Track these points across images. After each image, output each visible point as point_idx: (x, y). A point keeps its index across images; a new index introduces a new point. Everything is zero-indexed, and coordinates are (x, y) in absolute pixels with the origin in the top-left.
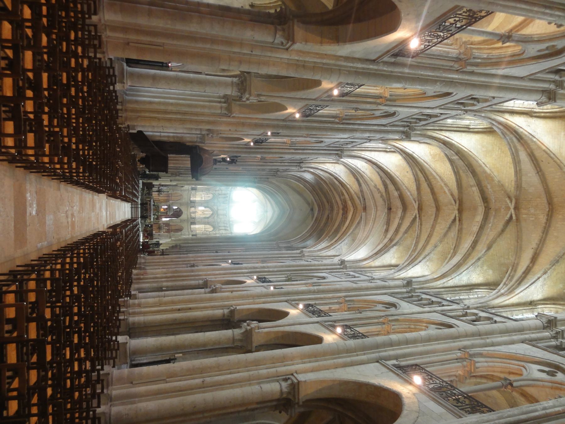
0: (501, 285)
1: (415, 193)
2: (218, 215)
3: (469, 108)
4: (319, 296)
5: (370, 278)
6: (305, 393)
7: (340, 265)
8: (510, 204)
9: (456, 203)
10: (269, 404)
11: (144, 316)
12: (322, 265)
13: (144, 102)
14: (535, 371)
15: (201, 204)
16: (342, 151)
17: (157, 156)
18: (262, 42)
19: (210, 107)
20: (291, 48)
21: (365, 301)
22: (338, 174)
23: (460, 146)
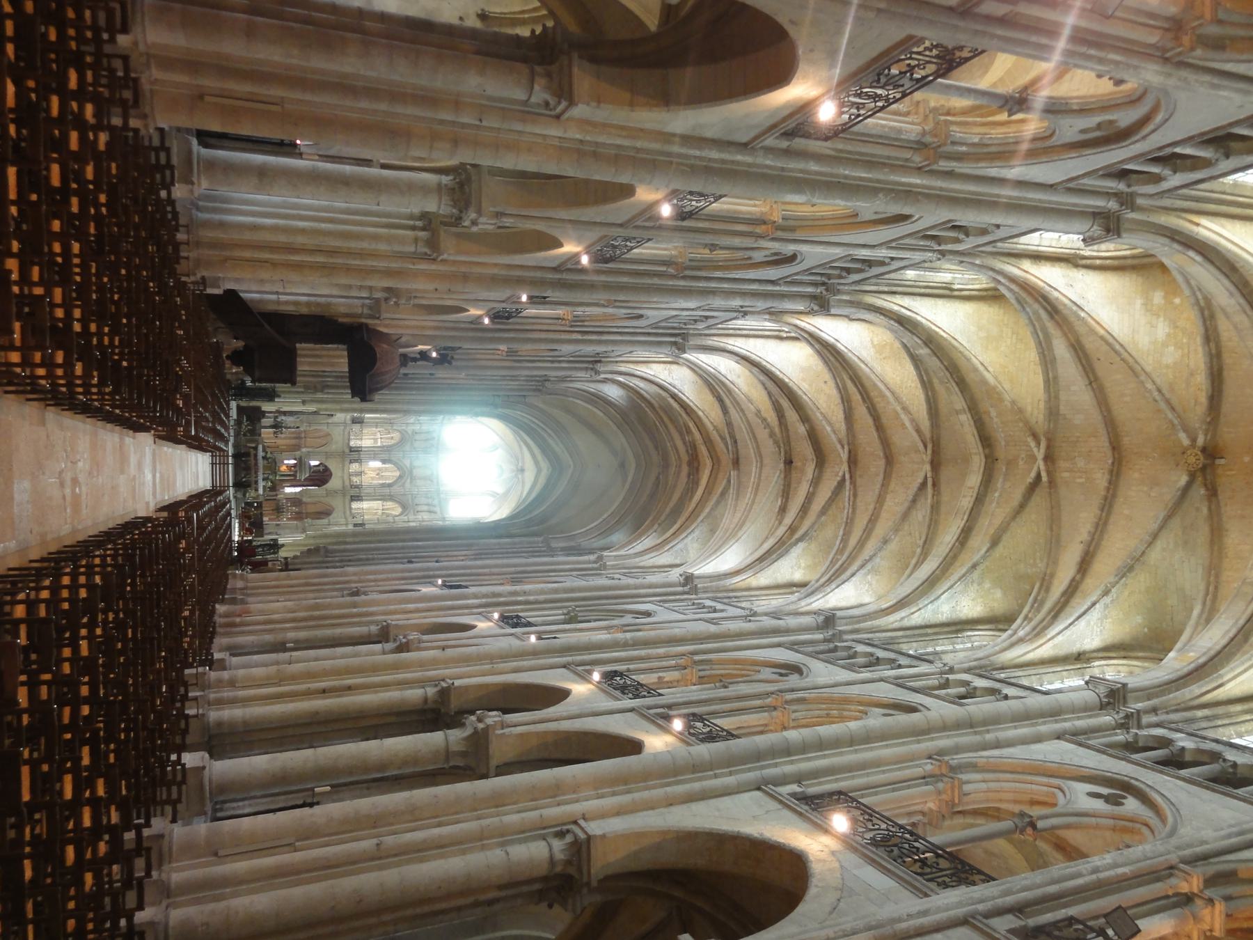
0: (1019, 621)
1: (842, 427)
2: (413, 479)
3: (949, 247)
4: (636, 653)
5: (748, 612)
6: (602, 862)
7: (684, 585)
8: (1035, 450)
9: (926, 447)
10: (525, 889)
11: (244, 706)
12: (643, 587)
13: (241, 227)
14: (1081, 796)
15: (374, 453)
16: (685, 336)
17: (270, 346)
18: (501, 100)
19: (389, 240)
20: (566, 115)
21: (736, 662)
22: (679, 386)
23: (934, 327)
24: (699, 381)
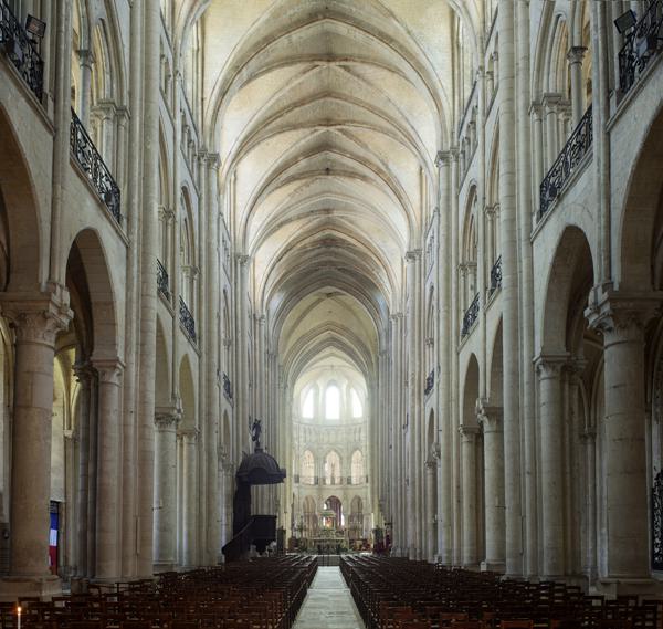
3: (171, 67)
24: (269, 239)
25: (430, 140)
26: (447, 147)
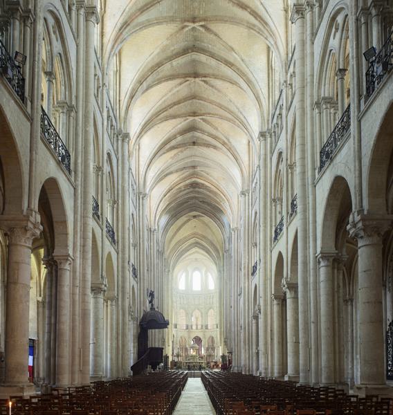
1: (178, 120)
25: (255, 125)
26: (265, 129)
